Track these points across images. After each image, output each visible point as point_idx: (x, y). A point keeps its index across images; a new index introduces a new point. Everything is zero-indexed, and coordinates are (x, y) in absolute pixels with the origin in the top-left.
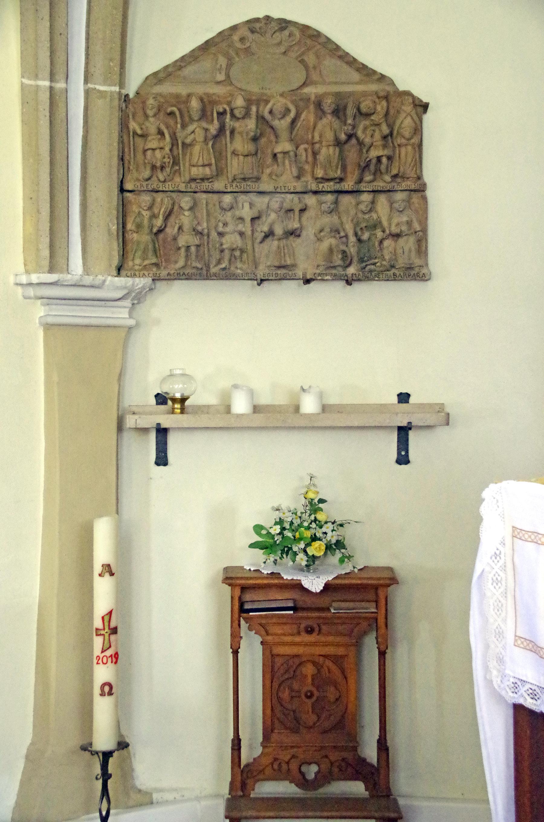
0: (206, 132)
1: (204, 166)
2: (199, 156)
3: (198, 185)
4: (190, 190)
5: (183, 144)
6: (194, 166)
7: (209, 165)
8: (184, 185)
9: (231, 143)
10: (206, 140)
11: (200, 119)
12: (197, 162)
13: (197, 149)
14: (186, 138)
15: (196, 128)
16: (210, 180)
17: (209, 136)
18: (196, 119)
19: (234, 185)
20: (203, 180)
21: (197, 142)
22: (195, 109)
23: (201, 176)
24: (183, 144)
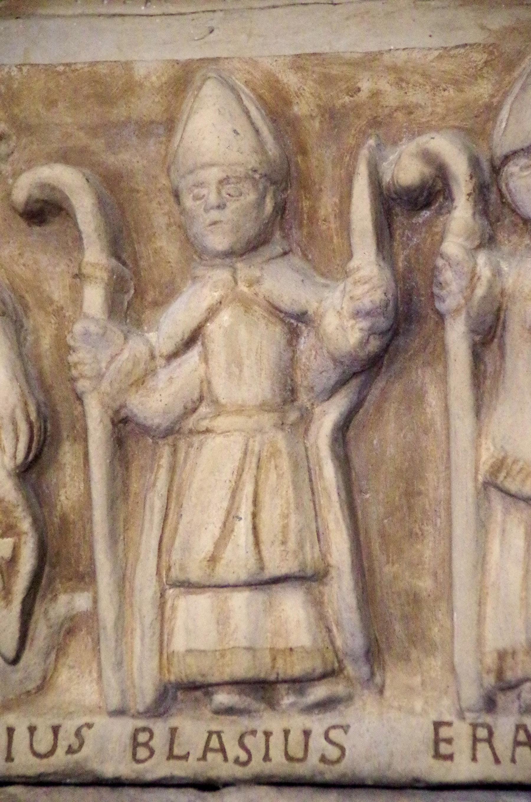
0: (293, 335)
1: (265, 583)
2: (231, 516)
3: (230, 730)
4: (159, 768)
5: (124, 429)
6: (188, 586)
7: (310, 579)
8: (124, 728)
9: (479, 408)
10: (288, 397)
11: (252, 246)
12: (213, 560)
13: (215, 463)
14: (141, 380)
15: (212, 312)
16: (319, 692)
17: (315, 367)
18: (218, 241)
19: (505, 726)
20: (261, 688)
21: (219, 409)
22: (213, 175)
23: (241, 667)
24: (124, 429)
